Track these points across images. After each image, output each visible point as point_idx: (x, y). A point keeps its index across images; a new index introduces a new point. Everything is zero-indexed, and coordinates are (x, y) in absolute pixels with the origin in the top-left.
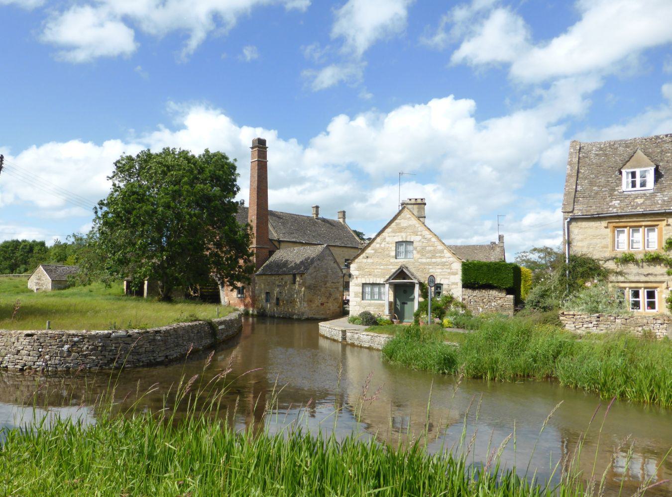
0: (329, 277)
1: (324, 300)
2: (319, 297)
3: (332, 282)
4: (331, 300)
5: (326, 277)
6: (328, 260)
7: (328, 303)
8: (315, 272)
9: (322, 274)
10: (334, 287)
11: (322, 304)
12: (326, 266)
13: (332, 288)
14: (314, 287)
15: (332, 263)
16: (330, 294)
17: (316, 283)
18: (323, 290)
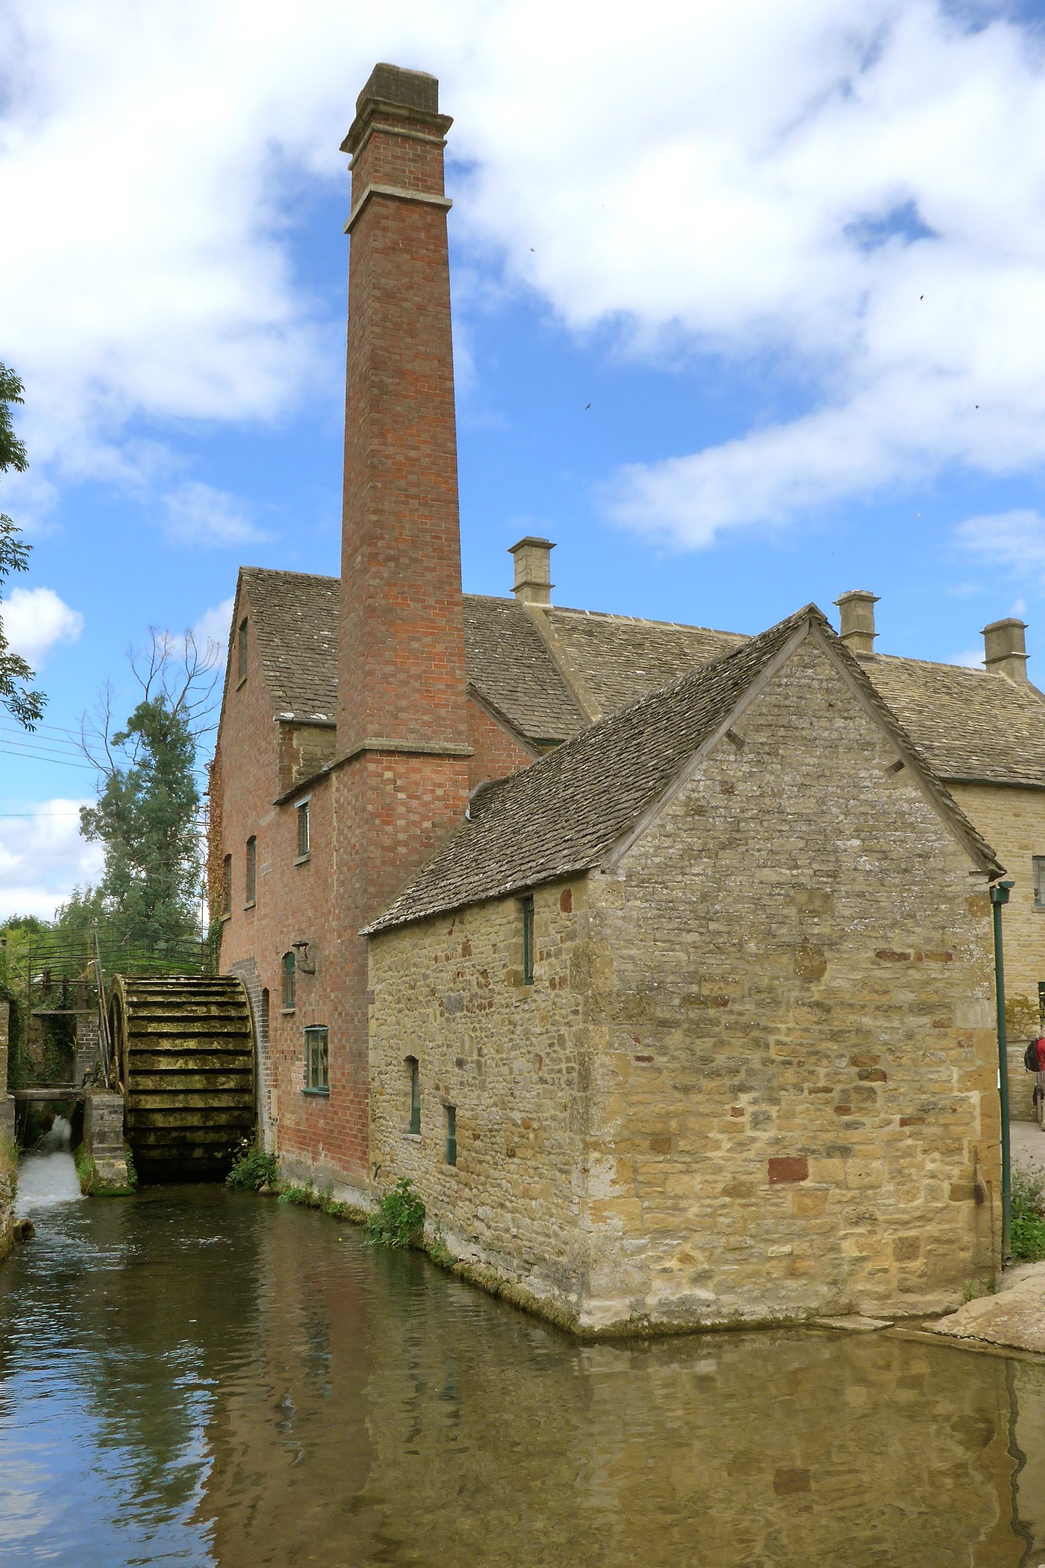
0: (844, 907)
1: (800, 1122)
2: (744, 1100)
3: (881, 954)
4: (878, 1123)
5: (818, 902)
6: (833, 746)
7: (845, 1151)
8: (691, 855)
9: (767, 874)
10: (907, 997)
11: (786, 1170)
12: (809, 805)
13: (888, 1010)
14: (689, 1000)
15: (872, 771)
16: (869, 1070)
17: (715, 965)
18: (789, 1026)
